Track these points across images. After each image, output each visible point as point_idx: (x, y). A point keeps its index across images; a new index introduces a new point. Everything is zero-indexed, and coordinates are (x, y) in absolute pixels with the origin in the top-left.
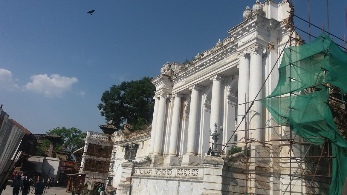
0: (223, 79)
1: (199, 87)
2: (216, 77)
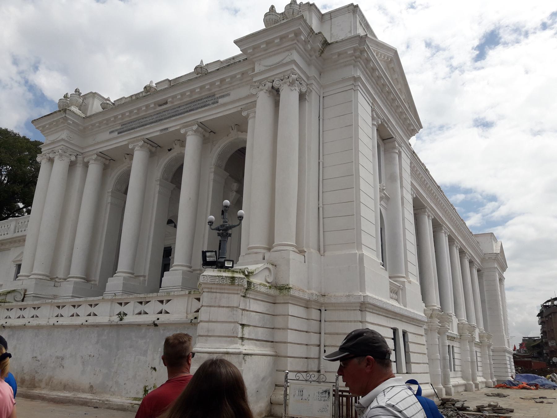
0: (207, 135)
1: (151, 147)
2: (195, 127)
